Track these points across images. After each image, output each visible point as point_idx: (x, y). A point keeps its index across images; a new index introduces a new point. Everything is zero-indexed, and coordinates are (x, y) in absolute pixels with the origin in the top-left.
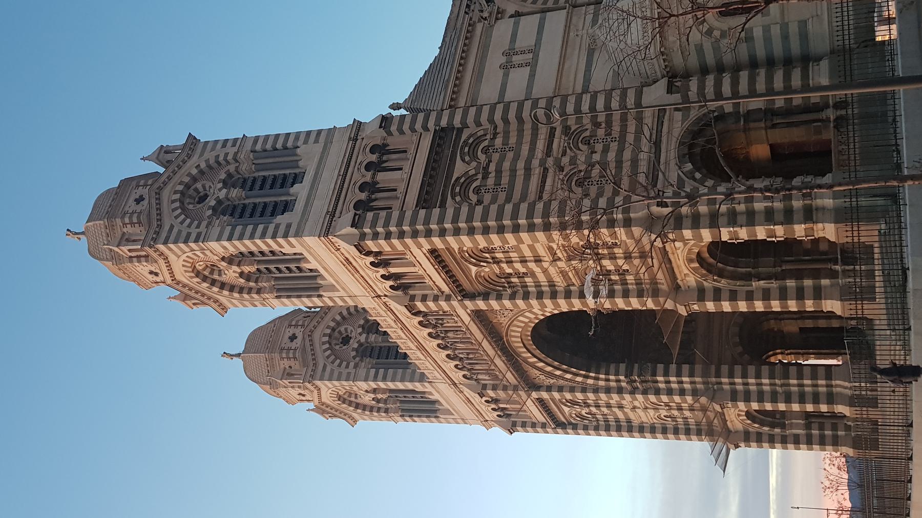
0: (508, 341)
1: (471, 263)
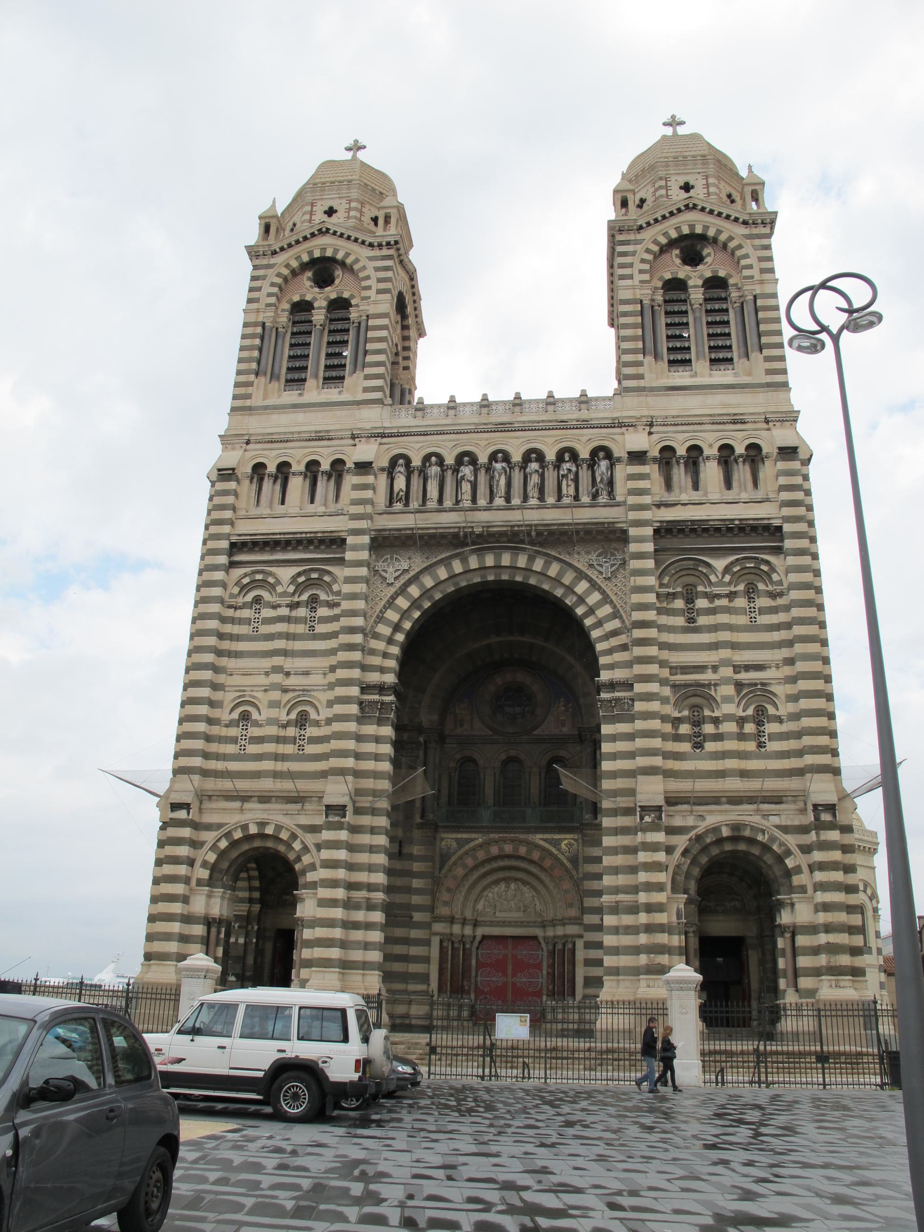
0: (524, 549)
1: (732, 563)
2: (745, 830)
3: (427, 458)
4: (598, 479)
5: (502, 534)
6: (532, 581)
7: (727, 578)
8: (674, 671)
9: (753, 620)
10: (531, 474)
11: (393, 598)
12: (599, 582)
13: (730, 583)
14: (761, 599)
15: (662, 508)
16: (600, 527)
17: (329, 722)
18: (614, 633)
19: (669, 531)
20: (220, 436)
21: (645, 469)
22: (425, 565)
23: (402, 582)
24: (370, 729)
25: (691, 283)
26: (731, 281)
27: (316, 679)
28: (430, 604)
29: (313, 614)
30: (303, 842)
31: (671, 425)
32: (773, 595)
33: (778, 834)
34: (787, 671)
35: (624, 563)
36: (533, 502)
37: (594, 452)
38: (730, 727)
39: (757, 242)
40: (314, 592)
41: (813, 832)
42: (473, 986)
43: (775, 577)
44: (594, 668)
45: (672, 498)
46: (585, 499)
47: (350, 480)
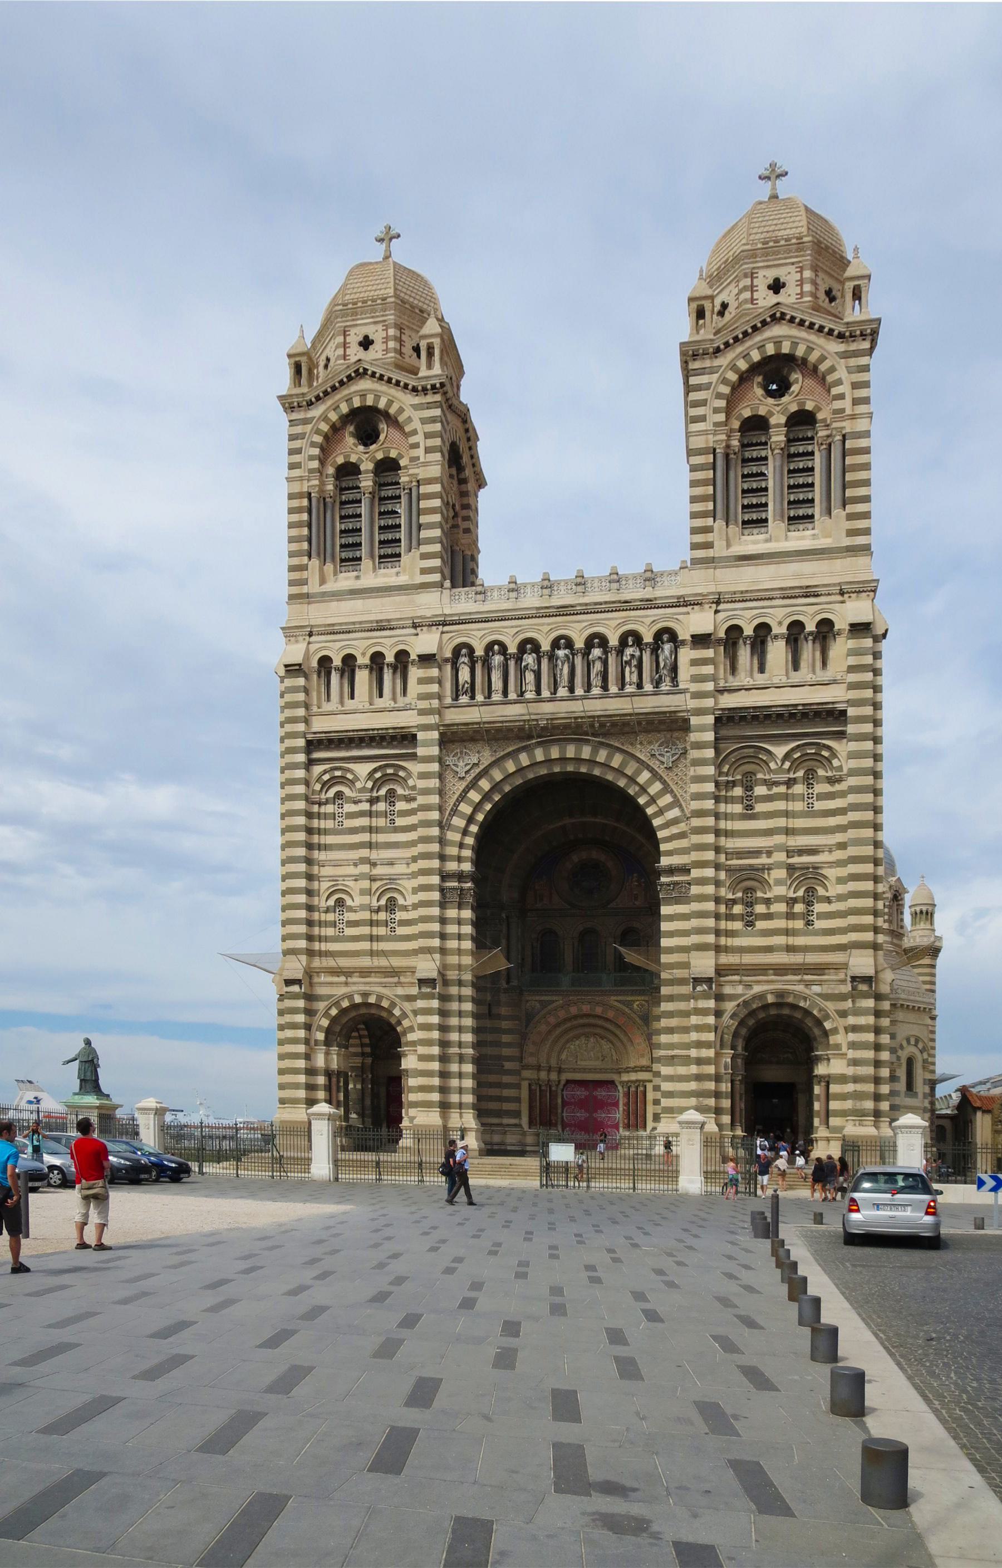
0: (587, 741)
1: (793, 750)
2: (788, 998)
3: (489, 648)
4: (662, 665)
5: (566, 726)
6: (597, 772)
7: (787, 765)
8: (729, 856)
9: (810, 805)
10: (594, 661)
11: (466, 791)
12: (660, 772)
13: (789, 770)
14: (820, 785)
15: (726, 694)
16: (662, 717)
17: (415, 906)
18: (675, 822)
19: (730, 719)
20: (282, 629)
21: (709, 653)
22: (494, 759)
23: (473, 775)
24: (452, 913)
25: (773, 421)
26: (820, 416)
27: (400, 869)
28: (500, 796)
29: (392, 808)
30: (401, 1009)
31: (739, 601)
32: (831, 781)
33: (819, 1001)
34: (839, 855)
35: (685, 753)
36: (596, 691)
37: (658, 636)
38: (781, 907)
39: (853, 362)
40: (391, 787)
41: (850, 1000)
42: (559, 1120)
43: (835, 763)
44: (657, 854)
45: (734, 682)
46: (648, 687)
47: (415, 673)
